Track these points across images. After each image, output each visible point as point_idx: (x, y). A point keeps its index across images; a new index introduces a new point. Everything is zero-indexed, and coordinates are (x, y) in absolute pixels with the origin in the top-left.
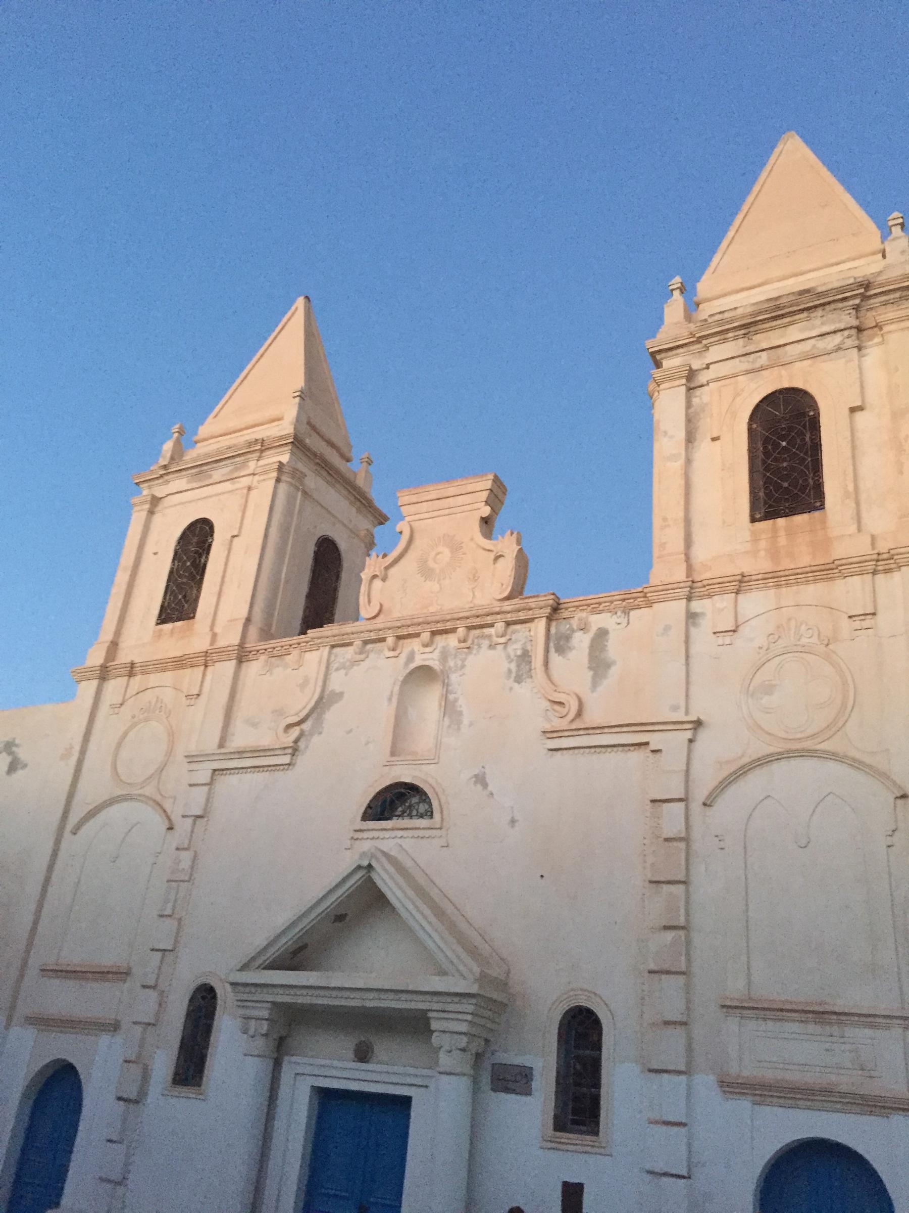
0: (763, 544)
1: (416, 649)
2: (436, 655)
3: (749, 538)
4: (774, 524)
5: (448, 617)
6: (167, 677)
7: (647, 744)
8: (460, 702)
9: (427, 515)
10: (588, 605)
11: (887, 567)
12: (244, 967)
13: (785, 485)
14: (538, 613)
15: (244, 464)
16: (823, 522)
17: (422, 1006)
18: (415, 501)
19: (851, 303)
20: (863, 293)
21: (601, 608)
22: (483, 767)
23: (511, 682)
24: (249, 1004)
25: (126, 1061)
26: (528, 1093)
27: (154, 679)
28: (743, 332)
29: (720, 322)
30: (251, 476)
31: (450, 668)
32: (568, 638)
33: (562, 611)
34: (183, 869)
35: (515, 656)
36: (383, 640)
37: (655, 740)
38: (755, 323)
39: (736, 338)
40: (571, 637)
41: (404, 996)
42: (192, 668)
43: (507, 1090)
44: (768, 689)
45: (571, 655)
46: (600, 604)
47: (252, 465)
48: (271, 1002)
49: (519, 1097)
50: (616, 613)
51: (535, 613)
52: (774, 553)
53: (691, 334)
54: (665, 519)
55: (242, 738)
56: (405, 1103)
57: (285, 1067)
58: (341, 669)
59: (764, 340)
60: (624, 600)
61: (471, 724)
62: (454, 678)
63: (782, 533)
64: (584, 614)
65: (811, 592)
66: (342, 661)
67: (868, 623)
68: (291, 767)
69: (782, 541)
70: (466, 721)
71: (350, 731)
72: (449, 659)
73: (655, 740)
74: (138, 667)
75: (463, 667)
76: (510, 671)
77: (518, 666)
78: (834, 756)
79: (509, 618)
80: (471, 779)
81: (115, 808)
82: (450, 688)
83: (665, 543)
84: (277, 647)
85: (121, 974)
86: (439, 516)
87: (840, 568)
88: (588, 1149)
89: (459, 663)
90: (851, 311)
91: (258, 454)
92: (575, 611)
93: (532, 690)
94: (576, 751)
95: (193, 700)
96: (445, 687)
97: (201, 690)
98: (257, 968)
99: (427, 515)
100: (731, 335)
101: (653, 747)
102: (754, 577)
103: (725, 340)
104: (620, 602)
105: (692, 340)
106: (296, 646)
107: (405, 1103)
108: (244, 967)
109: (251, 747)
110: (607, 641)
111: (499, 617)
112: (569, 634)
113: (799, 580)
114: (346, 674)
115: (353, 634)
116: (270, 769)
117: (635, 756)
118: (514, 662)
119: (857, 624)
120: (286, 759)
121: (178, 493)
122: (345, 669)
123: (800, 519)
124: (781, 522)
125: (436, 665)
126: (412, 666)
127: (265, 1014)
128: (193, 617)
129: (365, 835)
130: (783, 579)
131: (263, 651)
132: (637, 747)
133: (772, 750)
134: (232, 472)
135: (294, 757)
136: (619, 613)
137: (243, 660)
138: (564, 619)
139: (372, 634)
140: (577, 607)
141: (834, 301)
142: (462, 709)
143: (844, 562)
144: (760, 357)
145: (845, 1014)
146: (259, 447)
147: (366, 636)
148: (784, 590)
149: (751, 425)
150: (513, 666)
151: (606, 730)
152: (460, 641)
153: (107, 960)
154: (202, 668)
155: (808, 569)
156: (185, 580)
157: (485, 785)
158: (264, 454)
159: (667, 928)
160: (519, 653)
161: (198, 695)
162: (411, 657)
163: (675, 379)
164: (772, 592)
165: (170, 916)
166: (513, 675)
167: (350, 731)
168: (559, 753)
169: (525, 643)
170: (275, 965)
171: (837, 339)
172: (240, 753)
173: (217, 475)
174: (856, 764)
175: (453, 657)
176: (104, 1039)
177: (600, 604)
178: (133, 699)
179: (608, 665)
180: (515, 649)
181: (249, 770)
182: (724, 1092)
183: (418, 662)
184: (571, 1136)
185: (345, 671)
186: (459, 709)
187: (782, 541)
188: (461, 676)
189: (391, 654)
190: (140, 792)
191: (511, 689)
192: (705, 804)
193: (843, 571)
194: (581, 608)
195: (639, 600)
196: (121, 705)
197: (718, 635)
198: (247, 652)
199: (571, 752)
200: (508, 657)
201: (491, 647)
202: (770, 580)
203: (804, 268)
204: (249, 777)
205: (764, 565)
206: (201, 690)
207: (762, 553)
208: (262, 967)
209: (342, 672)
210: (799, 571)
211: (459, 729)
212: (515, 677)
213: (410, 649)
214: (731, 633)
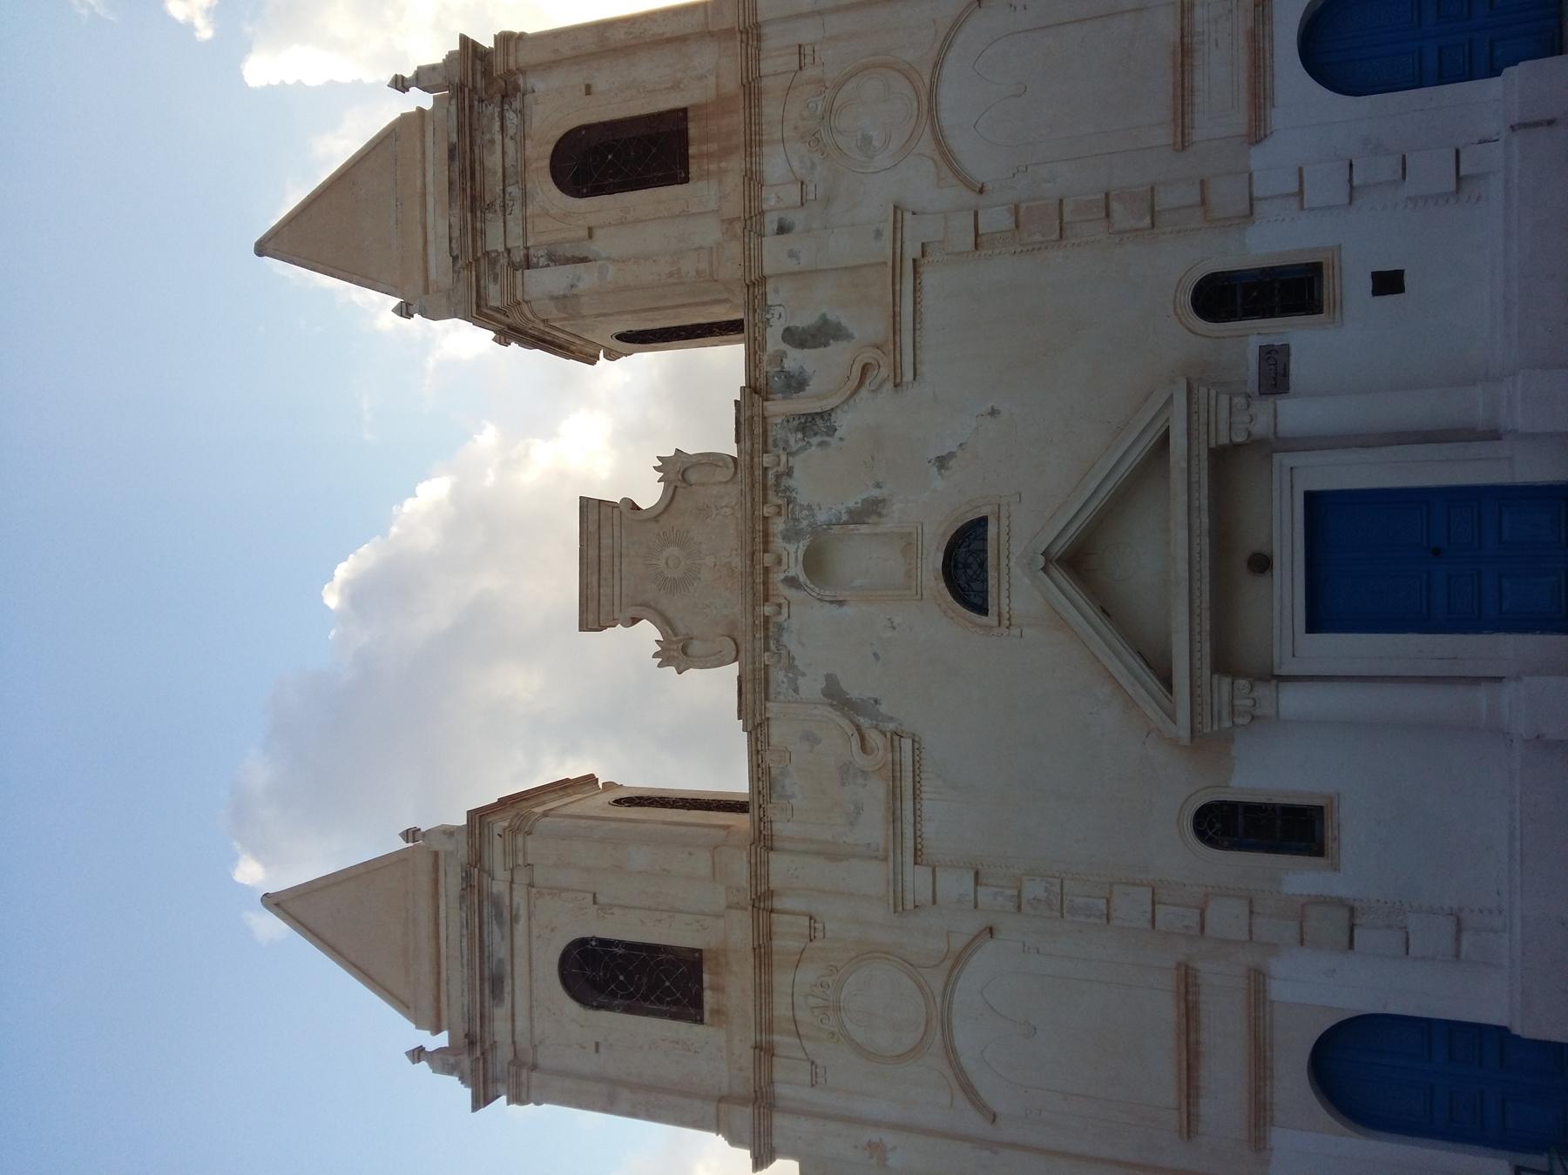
0: (713, 167)
1: (782, 576)
2: (792, 548)
3: (706, 182)
4: (694, 157)
5: (749, 523)
6: (782, 980)
7: (914, 260)
8: (851, 504)
9: (617, 588)
10: (755, 353)
11: (755, 37)
12: (1172, 716)
13: (654, 150)
14: (757, 410)
15: (496, 903)
16: (698, 107)
17: (1204, 455)
18: (596, 603)
19: (476, 103)
20: (469, 89)
21: (760, 338)
22: (929, 462)
23: (833, 441)
24: (1215, 708)
25: (1302, 942)
26: (1286, 349)
27: (781, 1009)
28: (478, 213)
29: (463, 233)
30: (514, 886)
31: (810, 525)
32: (788, 376)
33: (758, 384)
34: (1047, 890)
35: (803, 439)
36: (767, 619)
37: (912, 251)
38: (473, 198)
39: (484, 221)
40: (789, 372)
41: (1195, 478)
42: (773, 937)
43: (1286, 374)
44: (867, 140)
45: (809, 369)
46: (755, 339)
47: (499, 886)
48: (1212, 674)
49: (1292, 359)
50: (768, 320)
51: (757, 414)
52: (726, 153)
53: (467, 266)
54: (671, 275)
55: (872, 830)
56: (1311, 498)
57: (1284, 671)
58: (796, 684)
59: (494, 186)
60: (755, 311)
61: (878, 486)
62: (822, 517)
63: (704, 148)
64: (765, 358)
65: (771, 109)
66: (785, 685)
67: (808, 50)
68: (917, 739)
69: (713, 147)
70: (875, 493)
71: (875, 655)
72: (801, 527)
73: (912, 251)
74: (761, 1040)
75: (810, 507)
76: (821, 444)
77: (816, 434)
78: (938, 64)
79: (759, 446)
80: (941, 474)
81: (960, 1041)
82: (834, 521)
83: (697, 271)
84: (758, 787)
85: (1188, 986)
86: (620, 570)
87: (750, 79)
88: (1337, 270)
89: (805, 512)
90: (484, 105)
91: (486, 875)
92: (760, 370)
93: (846, 412)
94: (918, 345)
95: (817, 925)
96: (832, 526)
97: (804, 914)
98: (1171, 701)
99: (617, 588)
100: (478, 225)
101: (918, 254)
102: (748, 166)
103: (483, 232)
104: (756, 315)
105: (474, 268)
106: (760, 757)
107: (1311, 498)
108: (1172, 716)
109: (888, 796)
110: (798, 327)
111: (756, 460)
112: (785, 377)
113: (757, 121)
114: (804, 675)
115: (755, 663)
116: (917, 772)
117: (929, 278)
118: (809, 440)
119: (809, 60)
120: (907, 744)
121: (513, 1020)
122: (798, 679)
123: (693, 131)
124: (692, 151)
125: (803, 544)
126: (803, 578)
127: (1226, 681)
128: (700, 951)
129: (1005, 609)
130: (753, 137)
131: (762, 810)
132: (917, 276)
133: (928, 130)
134: (501, 924)
135: (904, 735)
136: (768, 316)
137: (770, 845)
138: (767, 384)
139: (758, 636)
140: (756, 366)
141: (470, 118)
142: (859, 501)
143: (744, 75)
144: (510, 193)
145: (1182, 29)
146: (476, 870)
147: (760, 644)
148: (765, 138)
149: (583, 193)
150: (815, 440)
151: (897, 309)
152: (779, 514)
153: (1167, 1010)
154: (773, 915)
155: (747, 111)
156: (645, 980)
157: (952, 455)
158: (487, 868)
159: (1108, 215)
160: (800, 435)
161: (811, 918)
162: (792, 582)
163: (514, 283)
164: (765, 149)
165: (1108, 902)
166: (826, 439)
167: (875, 655)
168: (918, 366)
169: (790, 429)
170: (1167, 681)
171: (510, 115)
172: (897, 835)
173: (502, 952)
174: (947, 44)
175: (796, 523)
176: (1278, 991)
177: (755, 339)
178: (806, 1044)
179: (824, 321)
180: (794, 440)
181: (918, 806)
182: (1266, 136)
183: (797, 570)
184: (1325, 297)
185: (800, 677)
186: (859, 505)
187: (713, 147)
188: (820, 509)
189: (785, 611)
190: (938, 1000)
191: (841, 439)
192: (981, 191)
193: (754, 76)
194: (757, 362)
195: (756, 293)
196: (812, 1063)
197: (804, 201)
198: (760, 837)
199: (918, 352)
200: (803, 449)
201: (789, 472)
202: (753, 150)
203: (419, 183)
204: (926, 806)
205: (736, 164)
206: (804, 914)
207: (723, 165)
208: (1169, 695)
209: (801, 681)
210: (748, 121)
211: (883, 501)
212: (828, 435)
213: (780, 586)
214: (804, 187)
